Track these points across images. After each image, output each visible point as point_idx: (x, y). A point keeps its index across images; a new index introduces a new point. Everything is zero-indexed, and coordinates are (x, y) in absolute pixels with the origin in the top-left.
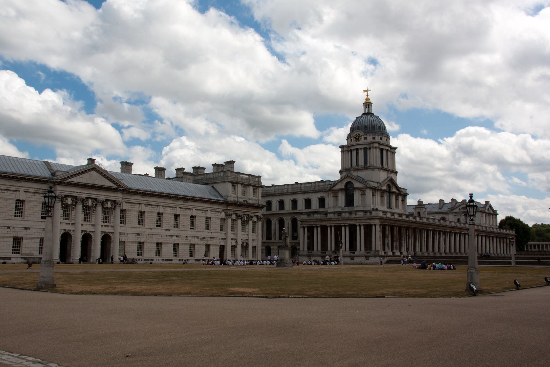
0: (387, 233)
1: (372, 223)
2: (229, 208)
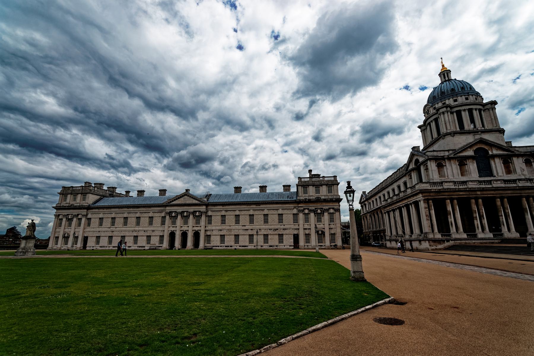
0: (450, 208)
1: (417, 200)
2: (299, 205)
